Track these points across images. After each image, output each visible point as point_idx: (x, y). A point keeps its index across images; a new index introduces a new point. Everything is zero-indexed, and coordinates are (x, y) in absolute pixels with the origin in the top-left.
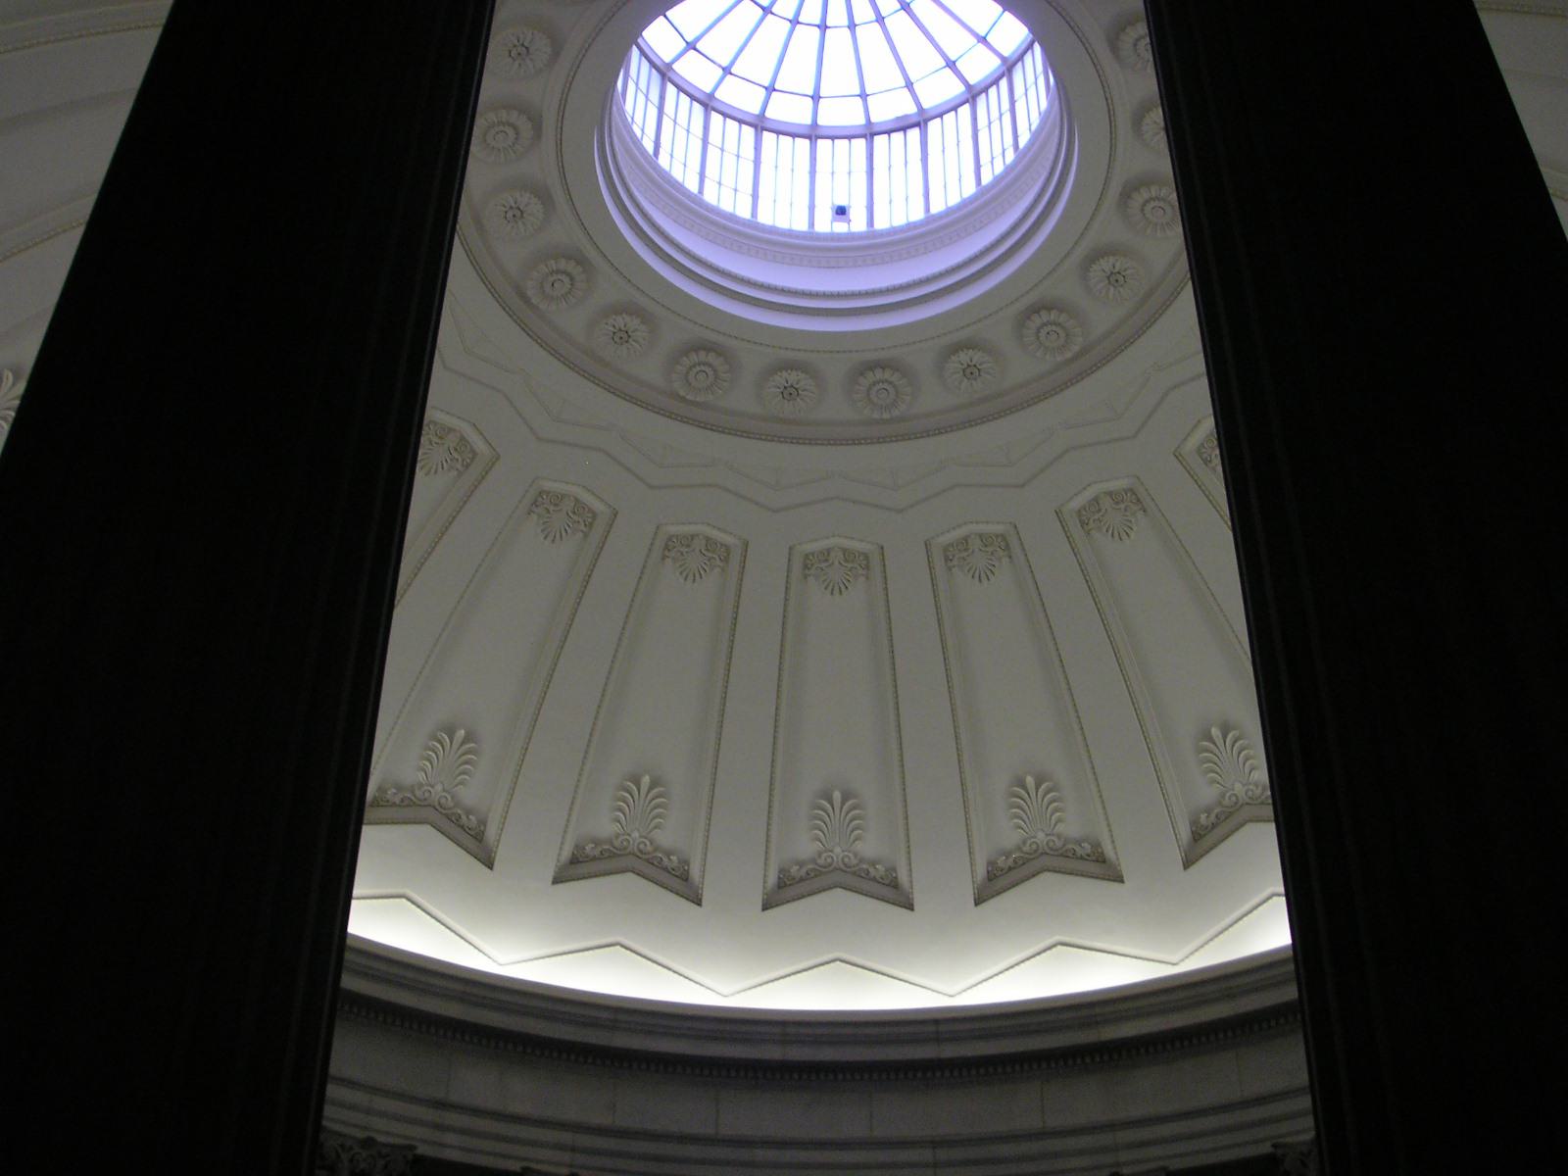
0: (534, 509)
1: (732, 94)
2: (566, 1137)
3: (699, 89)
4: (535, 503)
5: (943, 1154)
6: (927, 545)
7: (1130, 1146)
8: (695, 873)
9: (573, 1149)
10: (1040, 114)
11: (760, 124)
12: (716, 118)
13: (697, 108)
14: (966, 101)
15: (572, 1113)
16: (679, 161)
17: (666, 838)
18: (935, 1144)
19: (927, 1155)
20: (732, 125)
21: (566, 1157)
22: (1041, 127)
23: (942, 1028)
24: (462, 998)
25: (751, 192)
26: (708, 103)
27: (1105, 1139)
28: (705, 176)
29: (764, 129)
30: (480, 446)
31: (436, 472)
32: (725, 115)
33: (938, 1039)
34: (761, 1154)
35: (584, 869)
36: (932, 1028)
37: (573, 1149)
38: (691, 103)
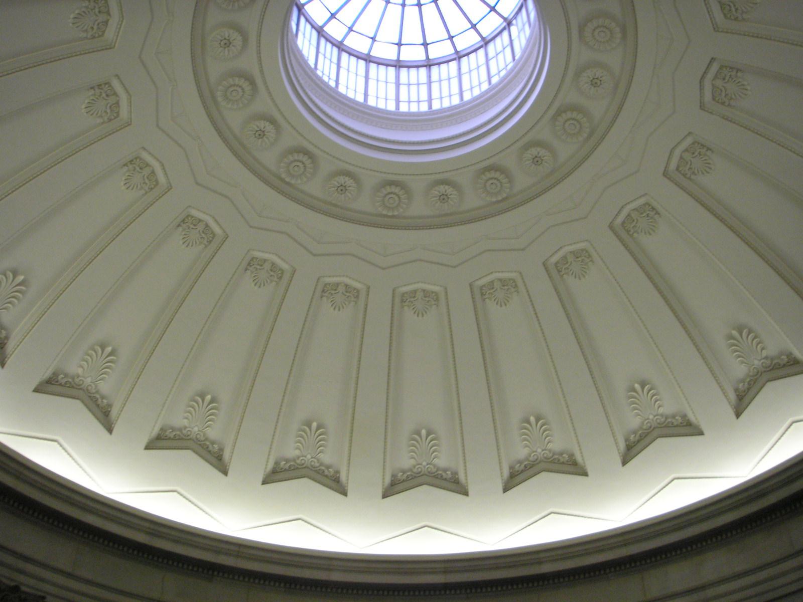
0: (249, 267)
1: (353, 42)
3: (336, 40)
4: (249, 264)
6: (471, 285)
8: (343, 477)
10: (521, 49)
11: (368, 59)
12: (345, 56)
13: (335, 50)
14: (481, 47)
16: (326, 70)
17: (327, 458)
20: (353, 59)
22: (526, 48)
25: (363, 92)
26: (340, 47)
28: (339, 84)
29: (370, 61)
30: (217, 230)
31: (192, 246)
32: (350, 54)
38: (332, 48)
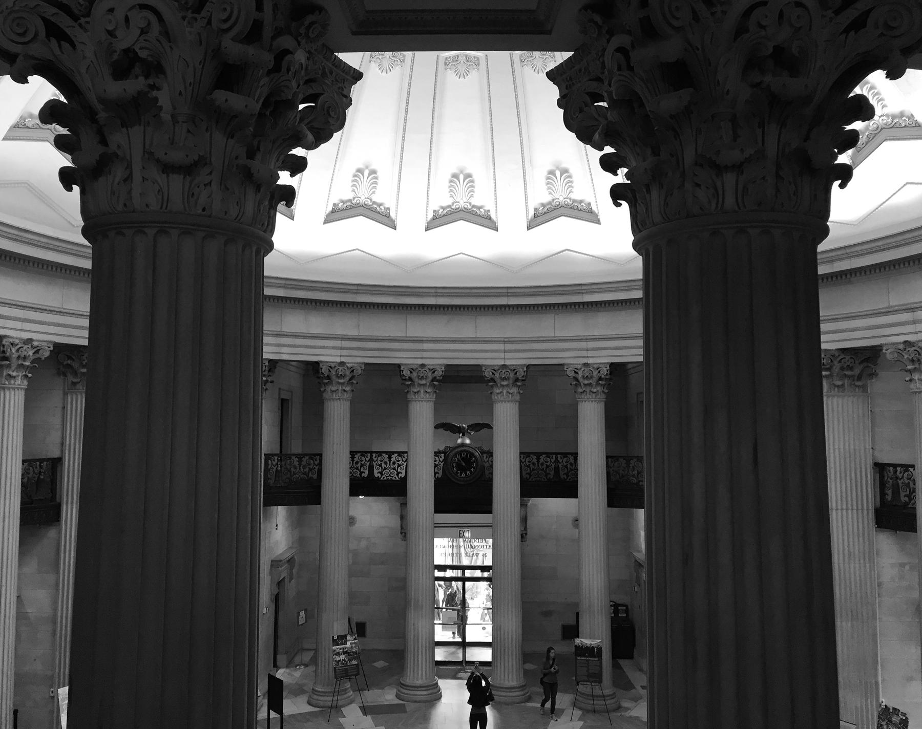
2: (338, 343)
5: (509, 347)
7: (594, 349)
9: (341, 348)
15: (339, 331)
18: (505, 341)
19: (501, 347)
21: (338, 352)
23: (510, 291)
24: (285, 287)
27: (583, 345)
33: (507, 295)
34: (426, 346)
35: (336, 215)
36: (505, 291)
37: (341, 348)
